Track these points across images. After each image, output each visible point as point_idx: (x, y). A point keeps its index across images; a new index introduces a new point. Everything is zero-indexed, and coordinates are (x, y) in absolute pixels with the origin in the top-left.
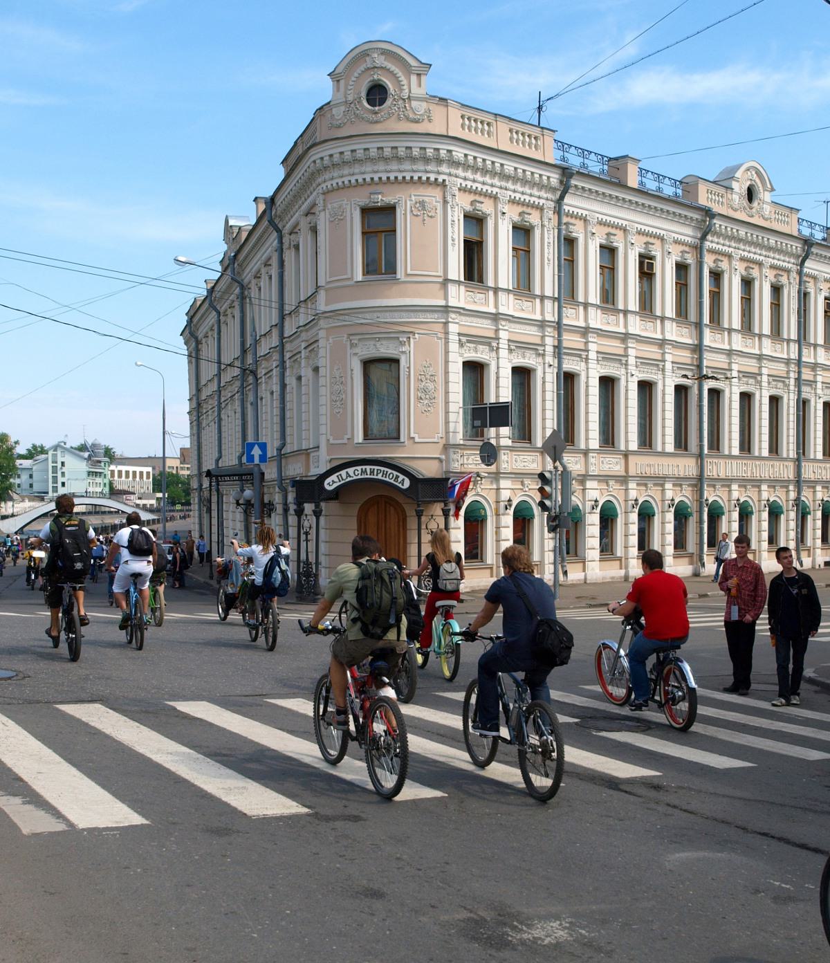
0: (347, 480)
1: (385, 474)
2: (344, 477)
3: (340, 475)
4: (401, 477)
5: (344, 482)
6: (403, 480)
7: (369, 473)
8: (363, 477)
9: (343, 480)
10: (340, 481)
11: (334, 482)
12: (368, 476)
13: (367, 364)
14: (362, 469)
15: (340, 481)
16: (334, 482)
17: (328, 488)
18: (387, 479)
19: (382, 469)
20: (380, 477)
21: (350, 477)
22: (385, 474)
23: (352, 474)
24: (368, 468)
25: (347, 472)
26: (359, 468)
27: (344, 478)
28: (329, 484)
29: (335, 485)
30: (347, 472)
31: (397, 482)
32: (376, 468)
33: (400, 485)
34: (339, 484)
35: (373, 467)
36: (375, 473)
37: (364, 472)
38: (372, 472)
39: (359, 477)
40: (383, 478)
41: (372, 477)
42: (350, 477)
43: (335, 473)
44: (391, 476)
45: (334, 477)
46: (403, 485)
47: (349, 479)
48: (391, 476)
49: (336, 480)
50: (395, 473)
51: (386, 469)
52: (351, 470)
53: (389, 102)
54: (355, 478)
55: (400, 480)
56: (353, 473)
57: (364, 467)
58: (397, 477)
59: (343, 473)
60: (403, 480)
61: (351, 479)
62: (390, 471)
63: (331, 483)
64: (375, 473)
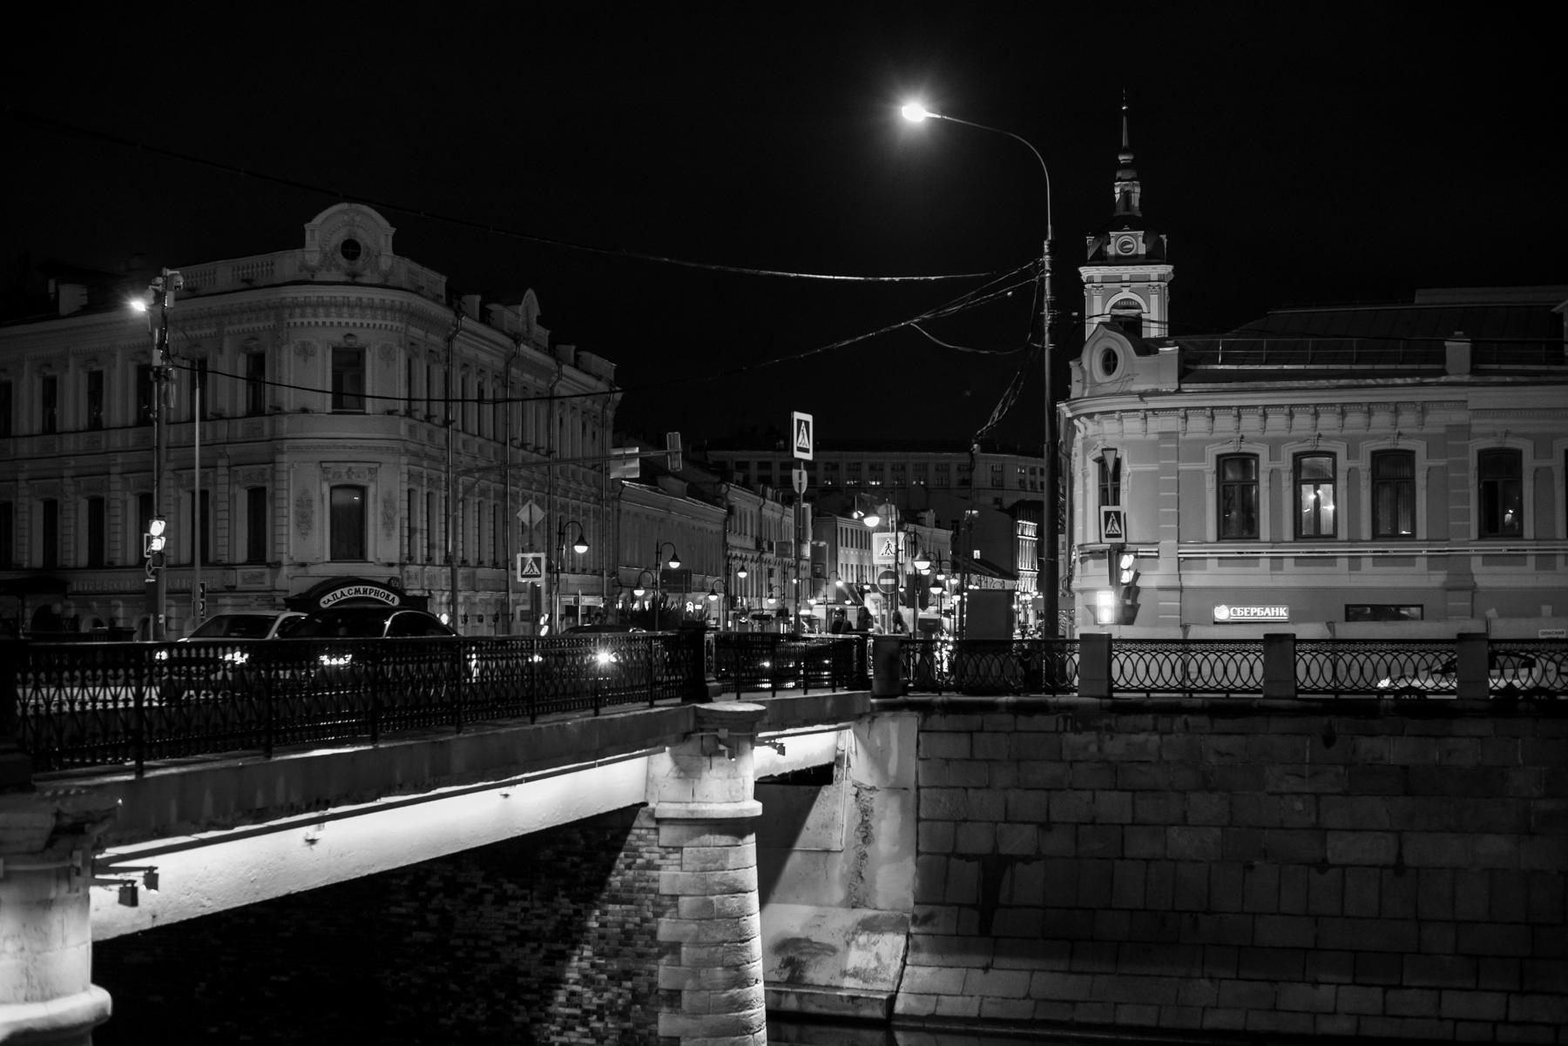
1: (377, 593)
4: (392, 596)
11: (329, 601)
13: (332, 489)
16: (329, 601)
18: (379, 598)
20: (372, 595)
22: (377, 593)
24: (362, 588)
26: (353, 588)
29: (330, 603)
32: (369, 587)
37: (357, 591)
38: (365, 591)
45: (329, 596)
47: (343, 598)
50: (386, 592)
52: (345, 590)
53: (362, 256)
56: (348, 592)
58: (388, 596)
59: (338, 593)
62: (382, 591)
63: (327, 601)
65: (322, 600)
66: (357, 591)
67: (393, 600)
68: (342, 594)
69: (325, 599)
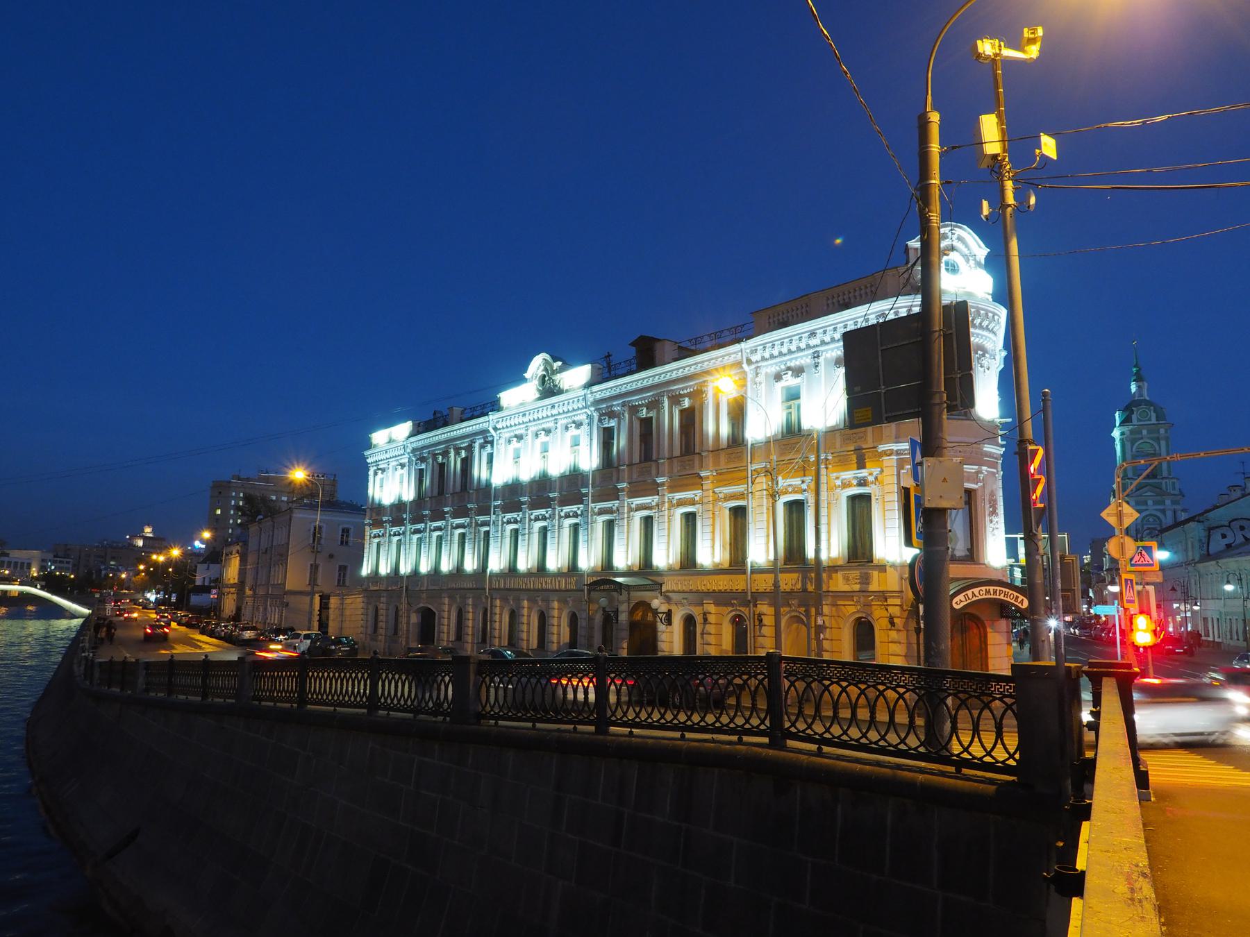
0: (973, 600)
1: (1006, 595)
2: (970, 597)
3: (967, 595)
4: (1021, 597)
5: (969, 601)
6: (1023, 600)
7: (992, 593)
8: (987, 597)
9: (969, 599)
10: (966, 600)
11: (961, 601)
12: (992, 596)
14: (986, 590)
15: (966, 600)
16: (961, 601)
17: (956, 606)
18: (1008, 599)
19: (1004, 589)
20: (1002, 597)
21: (976, 596)
22: (1006, 595)
23: (977, 594)
24: (992, 588)
25: (973, 592)
26: (984, 588)
27: (970, 597)
28: (956, 603)
29: (962, 604)
30: (973, 592)
31: (1017, 602)
32: (998, 588)
33: (1020, 605)
34: (966, 603)
35: (995, 588)
36: (998, 592)
37: (988, 592)
38: (995, 592)
39: (984, 597)
40: (1005, 599)
41: (995, 597)
42: (976, 596)
43: (962, 592)
44: (1011, 597)
45: (961, 597)
46: (1022, 605)
47: (975, 599)
48: (1011, 597)
49: (963, 599)
50: (1016, 594)
51: (1007, 590)
52: (976, 590)
54: (980, 597)
55: (1019, 600)
57: (988, 588)
58: (1017, 597)
59: (969, 592)
60: (1023, 600)
61: (977, 598)
62: (1011, 592)
64: (998, 592)
65: (954, 601)
66: (988, 592)
67: (1022, 602)
68: (974, 595)
69: (956, 599)
